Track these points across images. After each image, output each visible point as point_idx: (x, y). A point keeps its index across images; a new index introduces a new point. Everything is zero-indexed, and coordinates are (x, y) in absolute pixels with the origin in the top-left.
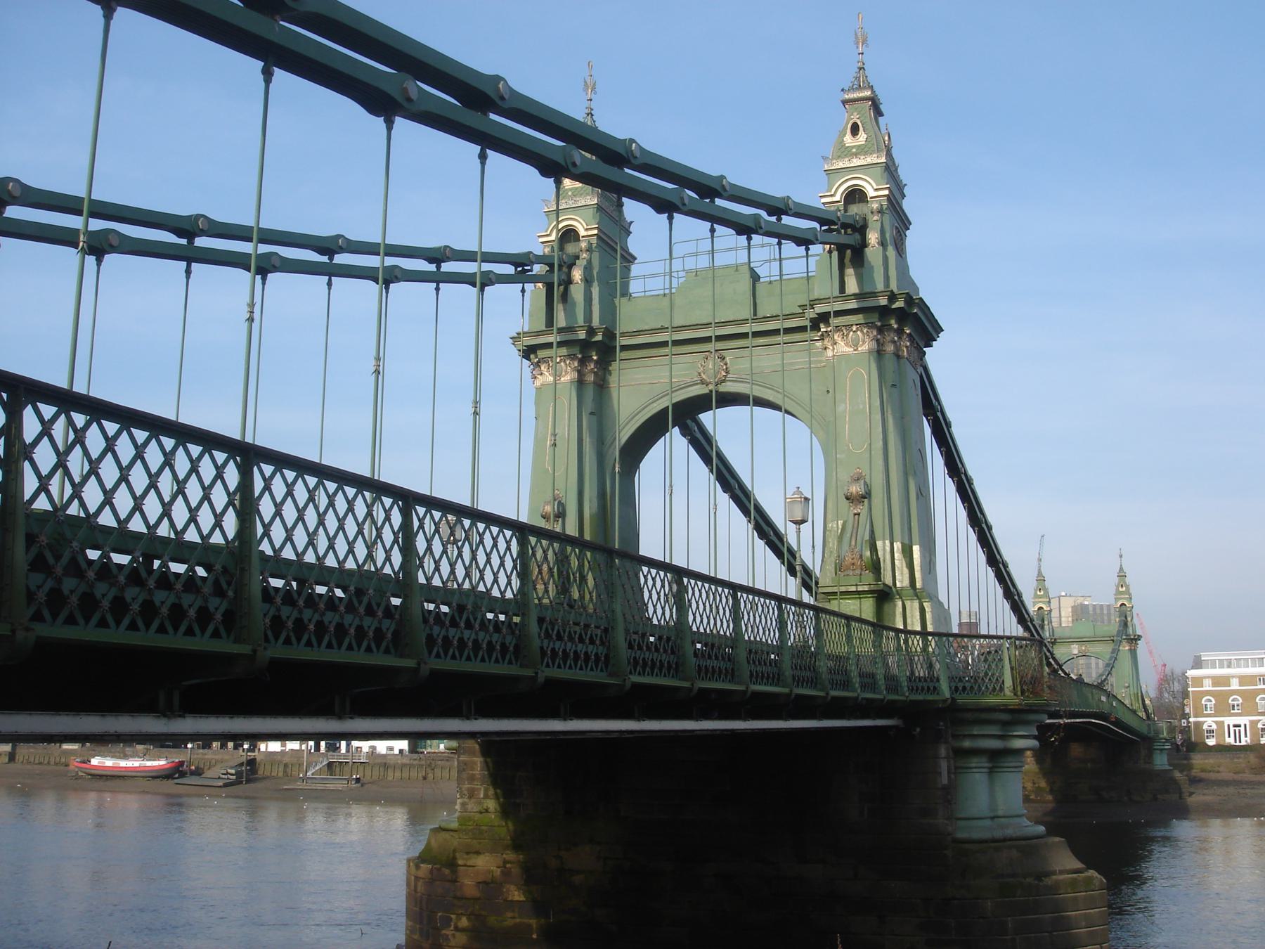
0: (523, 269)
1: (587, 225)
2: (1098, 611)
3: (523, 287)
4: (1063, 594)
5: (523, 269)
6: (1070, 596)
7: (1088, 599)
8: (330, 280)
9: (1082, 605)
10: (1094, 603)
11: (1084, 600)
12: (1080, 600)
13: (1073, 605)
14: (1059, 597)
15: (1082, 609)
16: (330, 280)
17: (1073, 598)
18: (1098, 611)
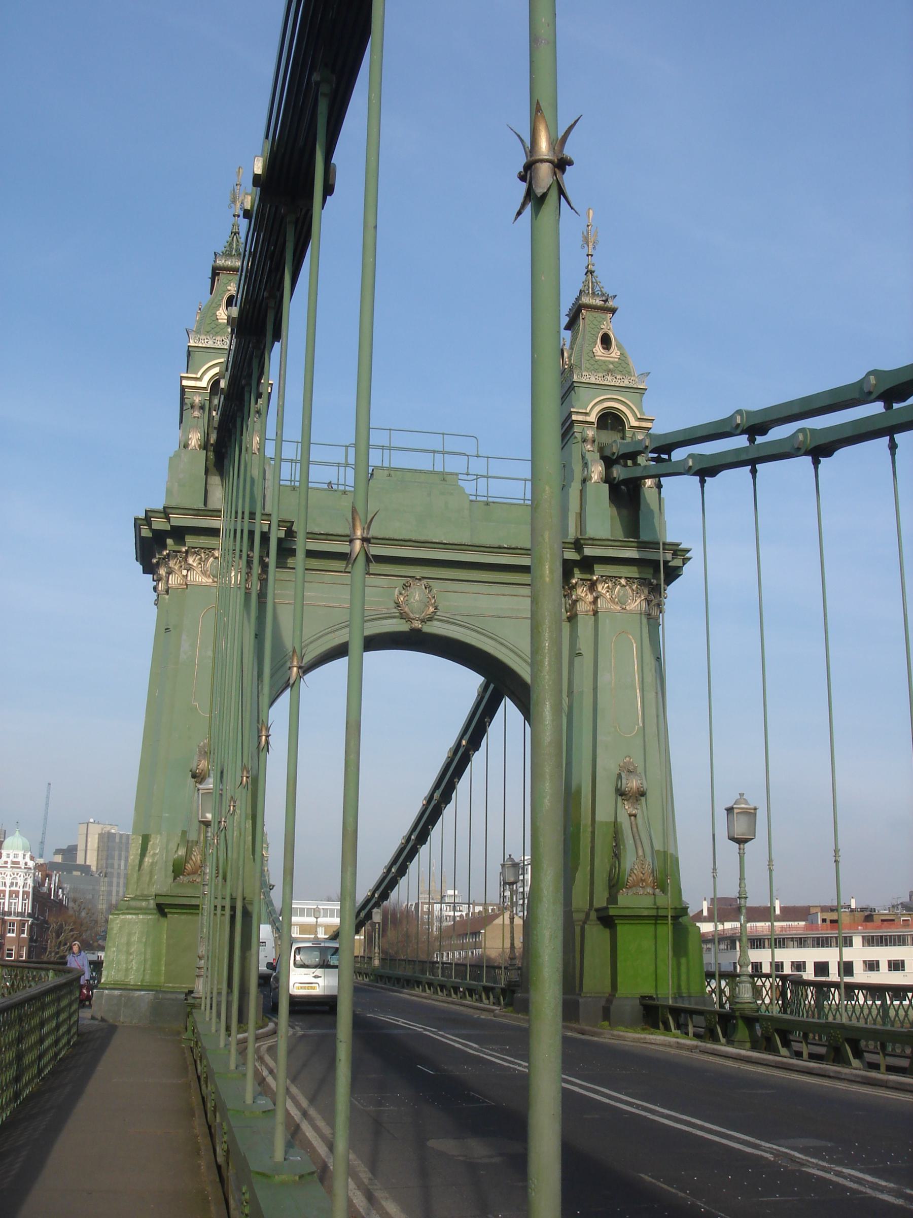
0: (659, 457)
1: (640, 415)
2: (124, 841)
3: (660, 481)
4: (92, 820)
5: (659, 457)
6: (98, 823)
7: (116, 827)
8: (892, 440)
9: (109, 833)
10: (121, 833)
11: (111, 829)
12: (108, 828)
13: (100, 832)
14: (88, 823)
15: (108, 837)
16: (892, 440)
17: (102, 826)
18: (124, 841)
